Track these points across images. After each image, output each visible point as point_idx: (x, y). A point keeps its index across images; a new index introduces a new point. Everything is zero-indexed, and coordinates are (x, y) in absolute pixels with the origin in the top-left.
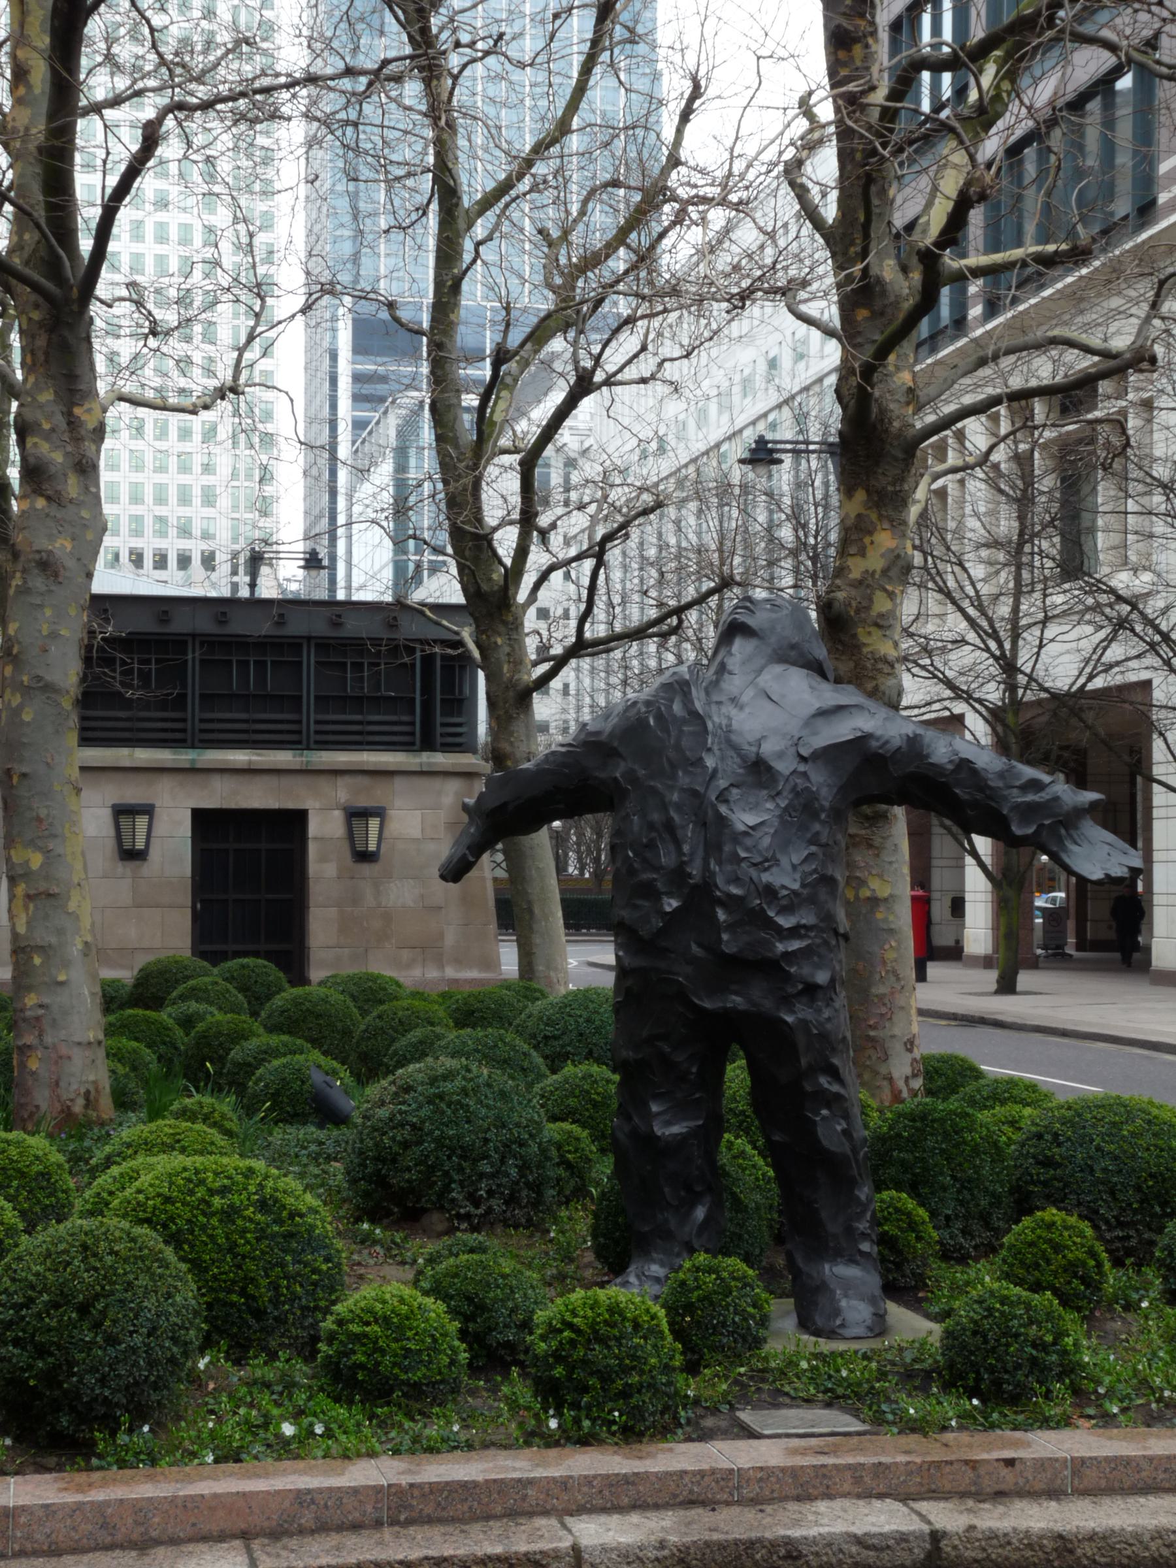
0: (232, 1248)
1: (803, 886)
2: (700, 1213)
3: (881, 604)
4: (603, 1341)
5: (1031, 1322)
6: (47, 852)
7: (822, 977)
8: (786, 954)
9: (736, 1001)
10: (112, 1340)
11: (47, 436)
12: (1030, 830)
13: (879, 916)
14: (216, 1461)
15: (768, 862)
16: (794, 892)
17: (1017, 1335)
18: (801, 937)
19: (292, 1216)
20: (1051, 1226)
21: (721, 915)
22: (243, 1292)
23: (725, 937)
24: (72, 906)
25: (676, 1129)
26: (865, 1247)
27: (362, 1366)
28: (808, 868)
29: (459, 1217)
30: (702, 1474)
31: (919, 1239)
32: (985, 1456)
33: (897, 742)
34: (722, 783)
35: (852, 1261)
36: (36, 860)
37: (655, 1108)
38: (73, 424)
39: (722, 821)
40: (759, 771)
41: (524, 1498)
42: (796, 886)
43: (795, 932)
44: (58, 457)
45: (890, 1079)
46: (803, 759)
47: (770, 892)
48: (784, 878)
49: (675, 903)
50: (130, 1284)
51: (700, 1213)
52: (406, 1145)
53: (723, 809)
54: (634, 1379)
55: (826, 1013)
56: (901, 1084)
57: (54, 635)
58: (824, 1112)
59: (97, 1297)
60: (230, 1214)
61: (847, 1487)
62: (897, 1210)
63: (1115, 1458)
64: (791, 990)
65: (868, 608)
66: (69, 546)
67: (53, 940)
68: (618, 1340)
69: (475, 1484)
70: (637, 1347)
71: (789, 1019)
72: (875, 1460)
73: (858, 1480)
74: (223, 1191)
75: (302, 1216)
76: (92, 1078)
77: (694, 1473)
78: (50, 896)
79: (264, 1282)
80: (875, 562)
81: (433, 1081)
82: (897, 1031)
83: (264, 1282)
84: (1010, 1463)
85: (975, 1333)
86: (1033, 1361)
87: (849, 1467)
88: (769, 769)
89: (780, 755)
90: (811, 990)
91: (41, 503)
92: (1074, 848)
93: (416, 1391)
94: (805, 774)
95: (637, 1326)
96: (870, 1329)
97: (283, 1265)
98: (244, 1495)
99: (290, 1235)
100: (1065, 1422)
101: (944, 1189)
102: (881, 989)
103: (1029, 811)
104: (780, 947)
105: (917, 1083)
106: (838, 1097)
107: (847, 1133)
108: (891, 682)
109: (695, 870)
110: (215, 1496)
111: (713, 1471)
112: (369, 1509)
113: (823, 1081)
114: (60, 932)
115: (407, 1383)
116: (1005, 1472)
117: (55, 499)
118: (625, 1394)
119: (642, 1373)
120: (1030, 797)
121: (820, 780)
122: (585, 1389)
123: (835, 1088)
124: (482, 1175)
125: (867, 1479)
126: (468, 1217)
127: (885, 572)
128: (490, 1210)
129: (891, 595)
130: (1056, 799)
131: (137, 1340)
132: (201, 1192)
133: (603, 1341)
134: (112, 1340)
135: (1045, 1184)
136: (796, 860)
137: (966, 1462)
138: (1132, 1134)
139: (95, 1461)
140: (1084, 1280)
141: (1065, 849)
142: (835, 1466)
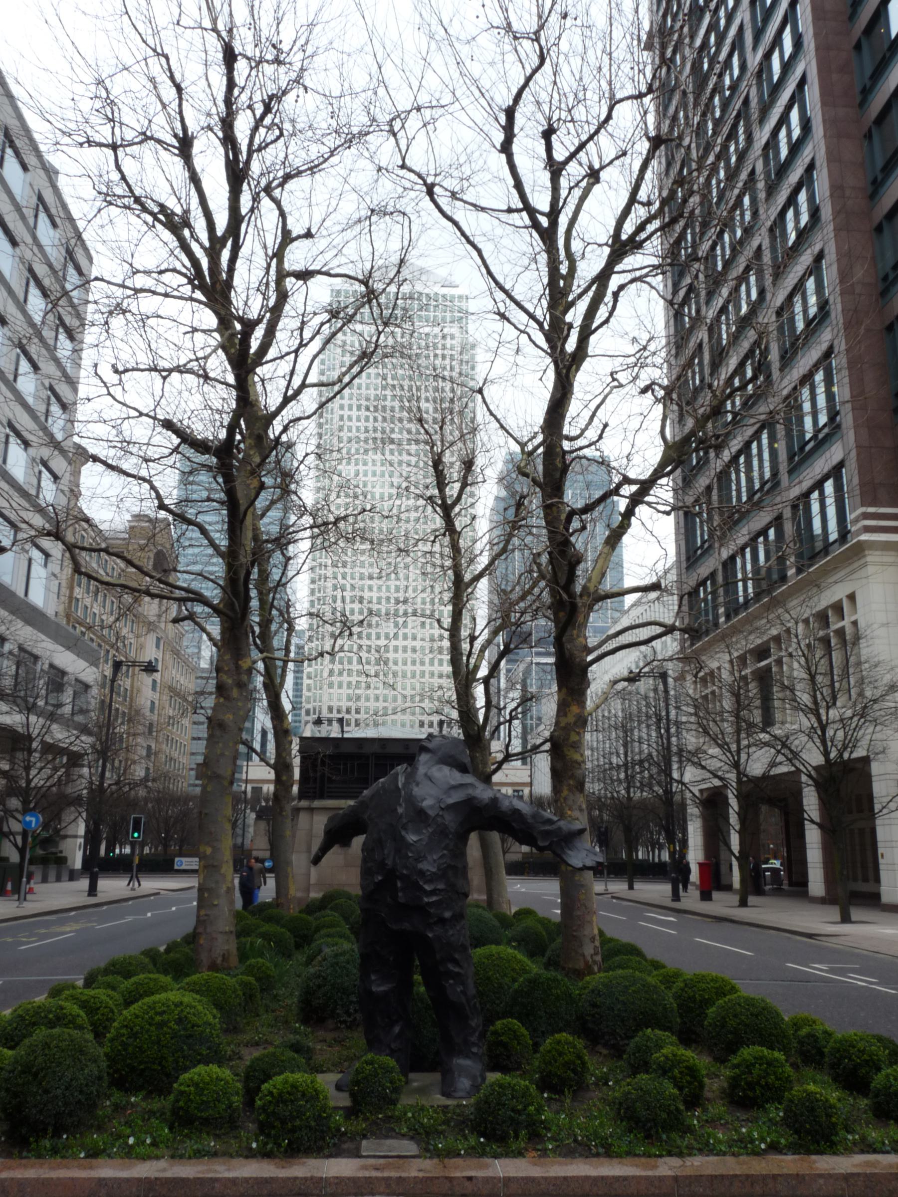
0: (159, 1042)
1: (439, 869)
2: (397, 1029)
3: (574, 737)
4: (285, 1102)
5: (513, 1097)
6: (213, 847)
7: (447, 914)
8: (428, 904)
9: (406, 926)
10: (46, 1092)
11: (226, 673)
12: (547, 844)
13: (577, 878)
14: (86, 1157)
15: (419, 859)
16: (434, 873)
17: (504, 1105)
18: (436, 895)
19: (193, 1026)
20: (559, 1042)
21: (399, 884)
22: (160, 1064)
23: (400, 894)
24: (223, 871)
25: (382, 988)
26: (475, 1050)
27: (182, 1108)
28: (441, 861)
29: (341, 1022)
30: (306, 1179)
31: (519, 1044)
32: (458, 1174)
33: (487, 801)
34: (404, 821)
35: (467, 1057)
36: (209, 851)
37: (373, 978)
38: (238, 667)
39: (403, 839)
40: (420, 816)
41: (213, 1188)
42: (434, 870)
43: (433, 892)
44: (230, 681)
45: (584, 956)
46: (442, 809)
47: (422, 873)
48: (429, 866)
49: (380, 878)
50: (60, 1063)
51: (397, 1029)
52: (319, 987)
53: (403, 833)
54: (298, 1123)
55: (451, 932)
56: (589, 958)
57: (222, 755)
58: (451, 982)
59: (42, 1069)
60: (161, 1025)
61: (382, 1189)
62: (510, 1029)
63: (526, 1178)
64: (431, 921)
65: (568, 739)
66: (231, 717)
67: (213, 885)
68: (292, 1101)
69: (188, 1179)
70: (301, 1106)
71: (430, 935)
72: (397, 1175)
73: (388, 1186)
74: (161, 1014)
75: (198, 1026)
76: (226, 947)
77: (302, 1178)
78: (214, 866)
79: (171, 1059)
80: (571, 719)
81: (336, 956)
82: (586, 933)
83: (171, 1059)
84: (470, 1179)
85: (486, 1102)
86: (512, 1119)
87: (383, 1178)
88: (426, 813)
89: (431, 807)
90: (442, 921)
91: (222, 700)
92: (569, 852)
93: (206, 1122)
94: (442, 816)
95: (304, 1095)
96: (468, 1093)
97: (182, 1050)
98: (72, 1179)
99: (191, 1036)
100: (520, 1154)
101: (541, 1017)
102: (578, 913)
103: (548, 833)
104: (426, 900)
105: (598, 958)
106: (458, 974)
107: (464, 992)
108: (580, 772)
109: (389, 862)
110: (58, 1179)
111: (312, 1178)
112: (134, 1190)
113: (451, 967)
114: (217, 882)
115: (201, 1118)
116: (467, 1184)
117: (228, 698)
118: (293, 1130)
119: (301, 1120)
120: (547, 828)
121: (449, 819)
122: (274, 1127)
123: (457, 970)
124: (352, 1002)
125: (393, 1186)
126: (345, 1022)
127: (575, 723)
128: (355, 1019)
129: (578, 733)
130: (560, 828)
131: (59, 1092)
132: (152, 1013)
133: (285, 1102)
134: (46, 1092)
135: (593, 1016)
136: (435, 857)
137: (446, 1178)
138: (634, 992)
139: (25, 1154)
140: (574, 1071)
141: (565, 853)
142: (376, 1178)
